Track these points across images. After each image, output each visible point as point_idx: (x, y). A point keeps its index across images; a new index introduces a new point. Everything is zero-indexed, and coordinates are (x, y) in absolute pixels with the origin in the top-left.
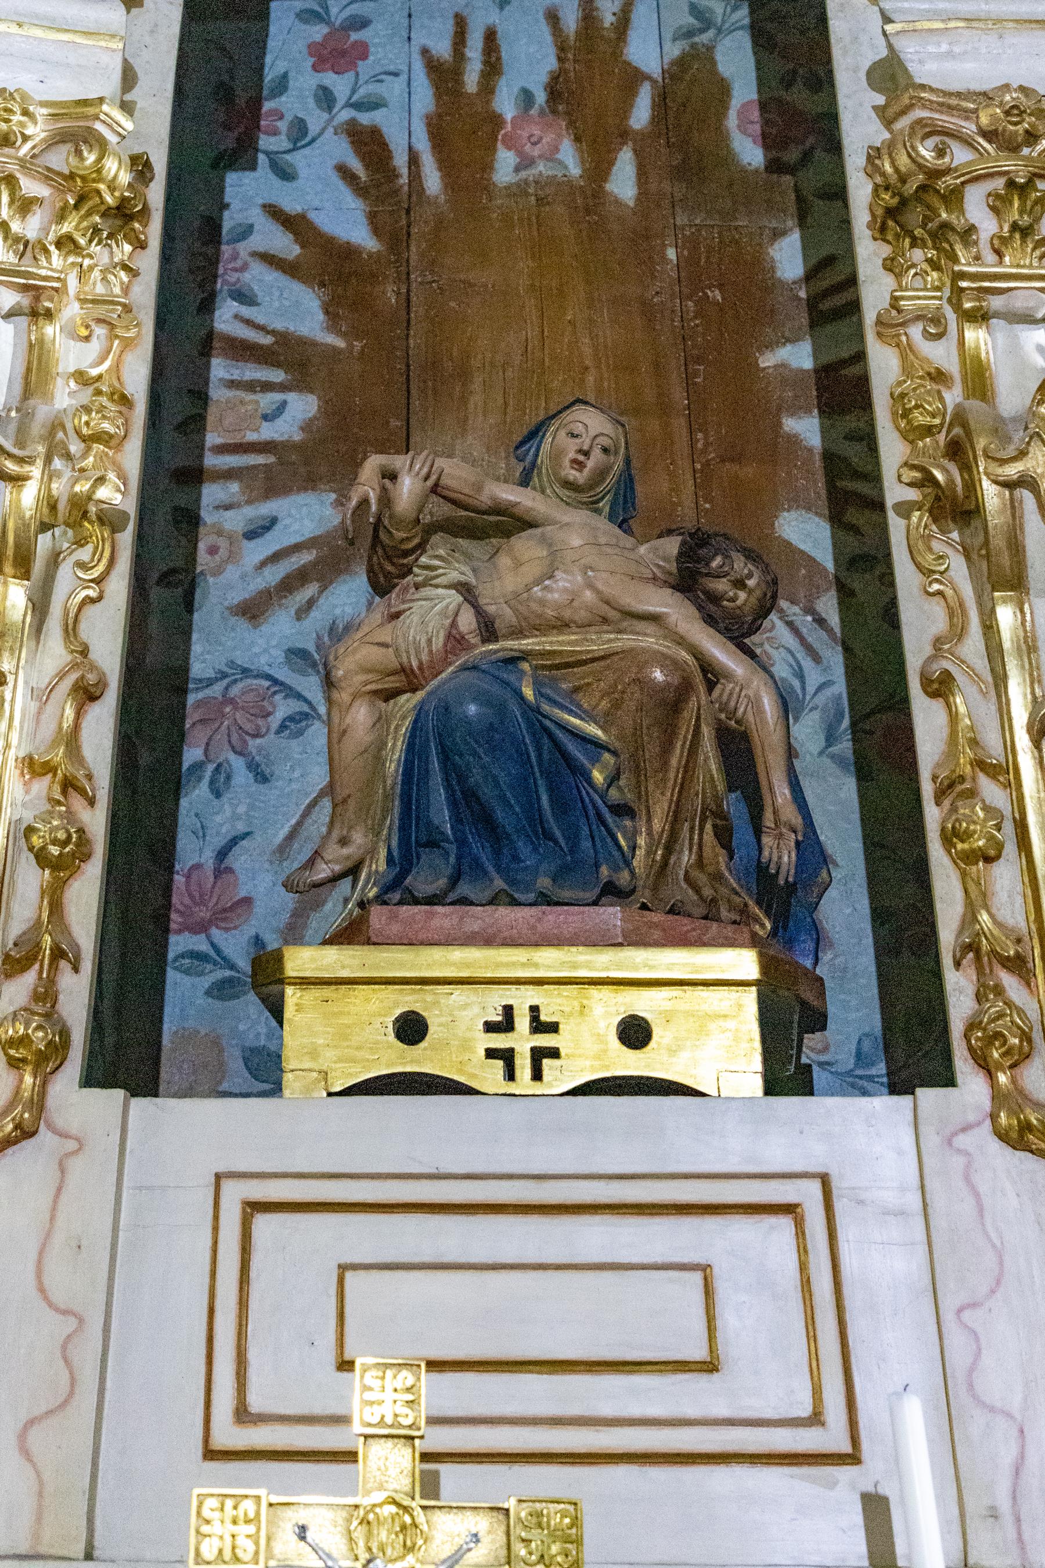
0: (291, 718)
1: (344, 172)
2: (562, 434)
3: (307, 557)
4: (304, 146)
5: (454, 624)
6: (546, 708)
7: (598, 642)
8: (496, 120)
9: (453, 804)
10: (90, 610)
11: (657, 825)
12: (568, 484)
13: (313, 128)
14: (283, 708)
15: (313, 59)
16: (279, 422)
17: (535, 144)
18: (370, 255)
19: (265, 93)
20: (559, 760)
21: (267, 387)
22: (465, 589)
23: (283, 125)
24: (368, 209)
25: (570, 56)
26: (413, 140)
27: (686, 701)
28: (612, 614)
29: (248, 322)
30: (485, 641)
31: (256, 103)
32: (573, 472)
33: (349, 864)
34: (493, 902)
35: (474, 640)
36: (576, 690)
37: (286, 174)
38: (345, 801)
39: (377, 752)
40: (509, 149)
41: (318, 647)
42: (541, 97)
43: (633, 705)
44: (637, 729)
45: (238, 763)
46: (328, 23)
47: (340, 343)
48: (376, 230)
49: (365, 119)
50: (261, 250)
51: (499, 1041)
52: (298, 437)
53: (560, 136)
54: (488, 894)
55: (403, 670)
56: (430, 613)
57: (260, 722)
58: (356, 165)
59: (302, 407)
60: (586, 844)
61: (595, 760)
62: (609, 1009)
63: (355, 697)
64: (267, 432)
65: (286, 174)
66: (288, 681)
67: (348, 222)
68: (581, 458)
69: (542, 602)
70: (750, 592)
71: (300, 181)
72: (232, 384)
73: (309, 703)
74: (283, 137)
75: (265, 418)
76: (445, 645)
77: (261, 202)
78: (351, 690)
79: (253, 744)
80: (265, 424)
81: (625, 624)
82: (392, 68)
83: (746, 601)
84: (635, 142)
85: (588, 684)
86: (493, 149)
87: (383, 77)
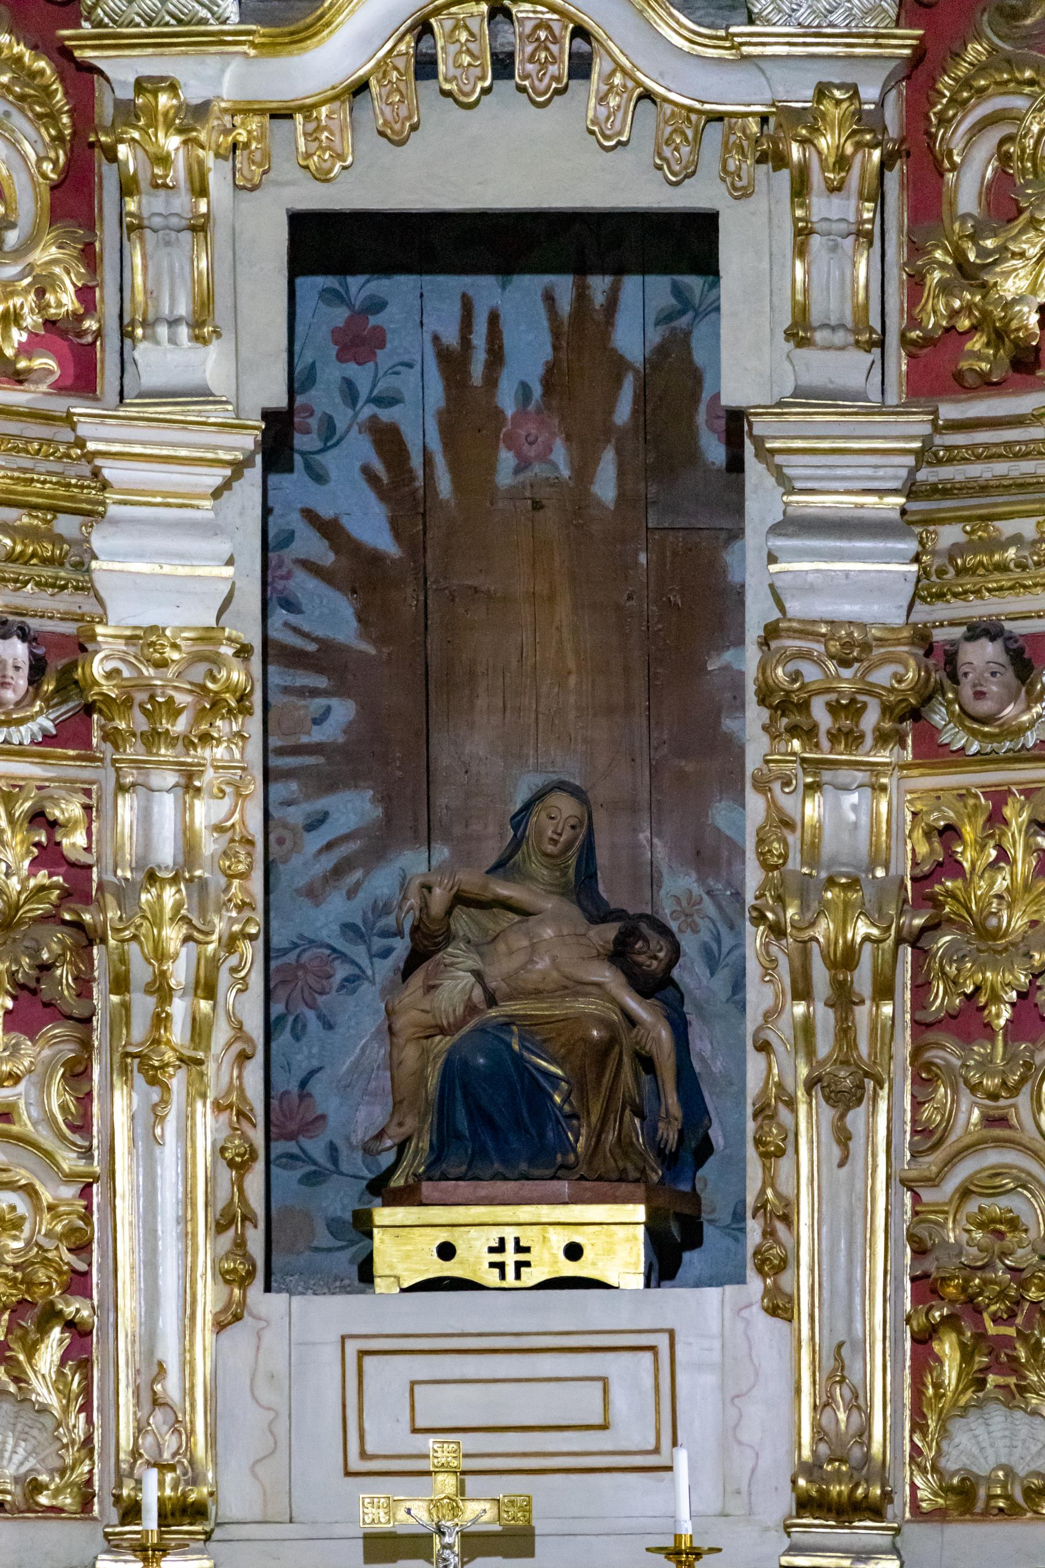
0: (346, 980)
1: (369, 475)
3: (353, 846)
5: (470, 998)
6: (526, 1054)
9: (470, 1115)
11: (594, 1119)
13: (341, 425)
14: (341, 972)
18: (393, 561)
20: (534, 1089)
22: (478, 975)
23: (313, 422)
27: (613, 1047)
28: (570, 984)
29: (296, 630)
30: (490, 1007)
33: (403, 1138)
34: (493, 1178)
35: (482, 1006)
36: (545, 1041)
37: (319, 477)
38: (401, 1102)
39: (421, 1076)
41: (365, 921)
43: (580, 1052)
44: (582, 1067)
45: (310, 1015)
46: (350, 306)
47: (372, 651)
49: (386, 415)
51: (496, 1258)
54: (490, 1173)
56: (455, 985)
57: (325, 982)
58: (378, 467)
60: (550, 1134)
65: (319, 477)
66: (343, 950)
67: (372, 526)
71: (332, 484)
73: (360, 968)
77: (299, 506)
79: (321, 999)
82: (406, 358)
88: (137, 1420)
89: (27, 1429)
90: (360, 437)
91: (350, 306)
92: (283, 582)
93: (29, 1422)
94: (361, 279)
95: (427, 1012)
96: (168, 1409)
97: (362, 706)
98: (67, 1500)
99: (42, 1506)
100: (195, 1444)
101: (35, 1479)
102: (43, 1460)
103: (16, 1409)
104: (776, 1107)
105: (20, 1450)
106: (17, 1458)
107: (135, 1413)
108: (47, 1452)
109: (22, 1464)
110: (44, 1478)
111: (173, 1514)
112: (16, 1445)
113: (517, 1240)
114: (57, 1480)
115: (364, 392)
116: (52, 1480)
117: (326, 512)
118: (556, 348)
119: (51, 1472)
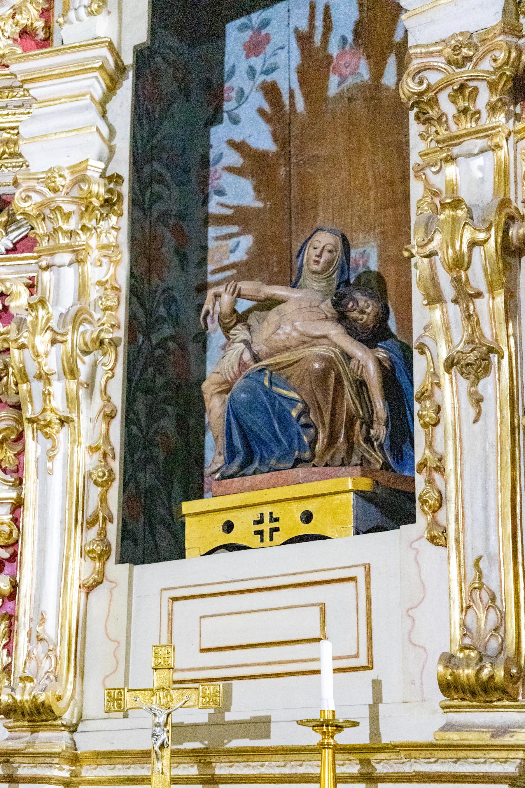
1: (261, 112)
2: (312, 247)
4: (243, 103)
5: (241, 359)
6: (275, 388)
7: (295, 355)
8: (329, 59)
10: (111, 381)
12: (314, 272)
13: (247, 91)
15: (245, 52)
16: (237, 252)
17: (347, 67)
19: (225, 78)
21: (231, 236)
23: (233, 94)
24: (271, 129)
25: (365, 8)
26: (291, 84)
29: (223, 205)
30: (256, 362)
31: (222, 85)
32: (315, 266)
35: (251, 363)
36: (288, 378)
37: (235, 121)
40: (335, 74)
42: (350, 37)
46: (252, 29)
48: (275, 139)
49: (269, 78)
50: (226, 165)
52: (245, 257)
53: (359, 59)
55: (226, 382)
58: (266, 107)
59: (246, 242)
61: (293, 406)
62: (297, 510)
63: (212, 396)
64: (233, 258)
65: (235, 121)
67: (262, 139)
68: (317, 259)
69: (275, 341)
70: (368, 315)
71: (242, 122)
72: (218, 238)
74: (234, 101)
75: (232, 252)
76: (239, 368)
77: (225, 139)
78: (209, 393)
80: (231, 255)
81: (314, 342)
82: (280, 45)
83: (367, 319)
84: (397, 49)
85: (292, 375)
86: (328, 77)
87: (278, 51)
90: (257, 94)
91: (252, 29)
92: (216, 182)
94: (258, 13)
95: (218, 373)
97: (256, 237)
104: (432, 391)
113: (271, 513)
115: (258, 70)
117: (238, 139)
118: (360, 12)
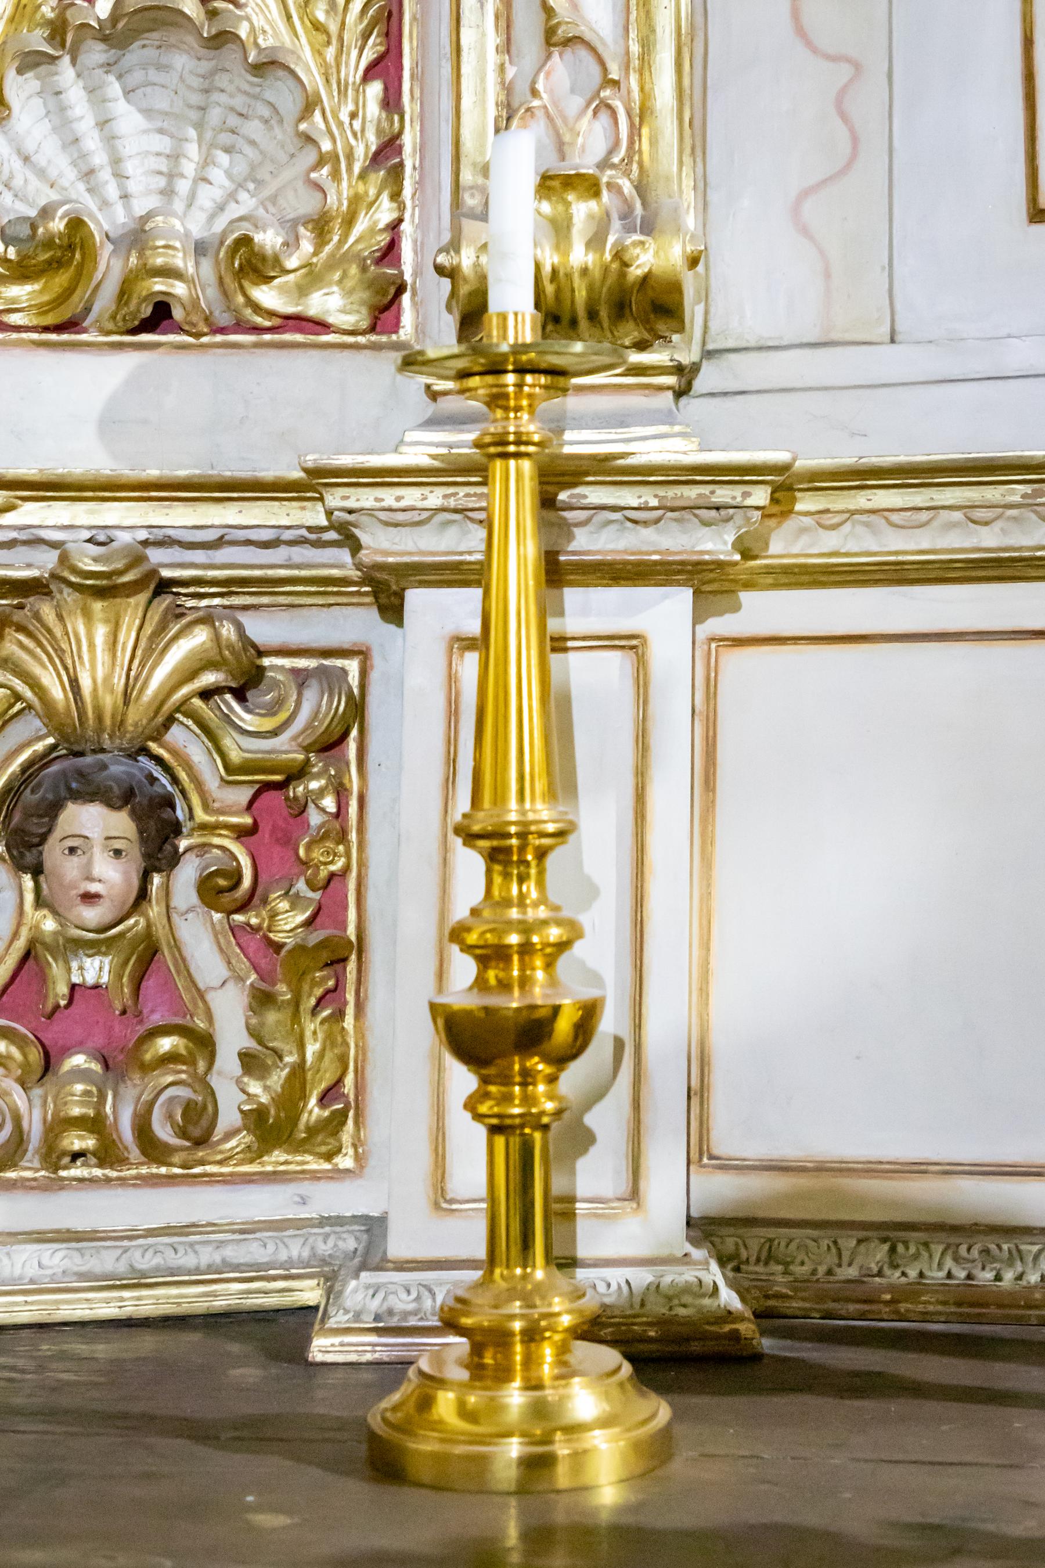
88: (508, 89)
89: (233, 121)
93: (239, 102)
96: (583, 53)
98: (330, 303)
99: (271, 314)
100: (654, 142)
101: (245, 241)
102: (274, 199)
103: (205, 66)
105: (217, 175)
106: (208, 197)
107: (502, 68)
108: (287, 174)
109: (221, 208)
110: (269, 239)
111: (592, 315)
112: (207, 162)
114: (307, 246)
116: (291, 244)
119: (291, 227)
